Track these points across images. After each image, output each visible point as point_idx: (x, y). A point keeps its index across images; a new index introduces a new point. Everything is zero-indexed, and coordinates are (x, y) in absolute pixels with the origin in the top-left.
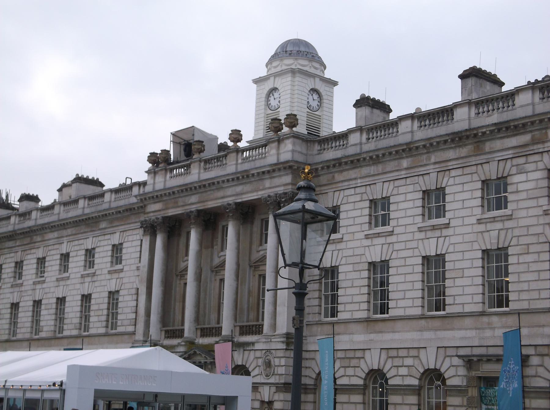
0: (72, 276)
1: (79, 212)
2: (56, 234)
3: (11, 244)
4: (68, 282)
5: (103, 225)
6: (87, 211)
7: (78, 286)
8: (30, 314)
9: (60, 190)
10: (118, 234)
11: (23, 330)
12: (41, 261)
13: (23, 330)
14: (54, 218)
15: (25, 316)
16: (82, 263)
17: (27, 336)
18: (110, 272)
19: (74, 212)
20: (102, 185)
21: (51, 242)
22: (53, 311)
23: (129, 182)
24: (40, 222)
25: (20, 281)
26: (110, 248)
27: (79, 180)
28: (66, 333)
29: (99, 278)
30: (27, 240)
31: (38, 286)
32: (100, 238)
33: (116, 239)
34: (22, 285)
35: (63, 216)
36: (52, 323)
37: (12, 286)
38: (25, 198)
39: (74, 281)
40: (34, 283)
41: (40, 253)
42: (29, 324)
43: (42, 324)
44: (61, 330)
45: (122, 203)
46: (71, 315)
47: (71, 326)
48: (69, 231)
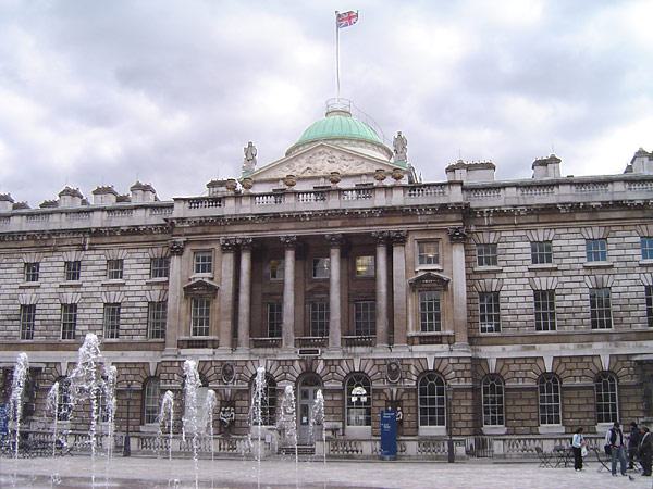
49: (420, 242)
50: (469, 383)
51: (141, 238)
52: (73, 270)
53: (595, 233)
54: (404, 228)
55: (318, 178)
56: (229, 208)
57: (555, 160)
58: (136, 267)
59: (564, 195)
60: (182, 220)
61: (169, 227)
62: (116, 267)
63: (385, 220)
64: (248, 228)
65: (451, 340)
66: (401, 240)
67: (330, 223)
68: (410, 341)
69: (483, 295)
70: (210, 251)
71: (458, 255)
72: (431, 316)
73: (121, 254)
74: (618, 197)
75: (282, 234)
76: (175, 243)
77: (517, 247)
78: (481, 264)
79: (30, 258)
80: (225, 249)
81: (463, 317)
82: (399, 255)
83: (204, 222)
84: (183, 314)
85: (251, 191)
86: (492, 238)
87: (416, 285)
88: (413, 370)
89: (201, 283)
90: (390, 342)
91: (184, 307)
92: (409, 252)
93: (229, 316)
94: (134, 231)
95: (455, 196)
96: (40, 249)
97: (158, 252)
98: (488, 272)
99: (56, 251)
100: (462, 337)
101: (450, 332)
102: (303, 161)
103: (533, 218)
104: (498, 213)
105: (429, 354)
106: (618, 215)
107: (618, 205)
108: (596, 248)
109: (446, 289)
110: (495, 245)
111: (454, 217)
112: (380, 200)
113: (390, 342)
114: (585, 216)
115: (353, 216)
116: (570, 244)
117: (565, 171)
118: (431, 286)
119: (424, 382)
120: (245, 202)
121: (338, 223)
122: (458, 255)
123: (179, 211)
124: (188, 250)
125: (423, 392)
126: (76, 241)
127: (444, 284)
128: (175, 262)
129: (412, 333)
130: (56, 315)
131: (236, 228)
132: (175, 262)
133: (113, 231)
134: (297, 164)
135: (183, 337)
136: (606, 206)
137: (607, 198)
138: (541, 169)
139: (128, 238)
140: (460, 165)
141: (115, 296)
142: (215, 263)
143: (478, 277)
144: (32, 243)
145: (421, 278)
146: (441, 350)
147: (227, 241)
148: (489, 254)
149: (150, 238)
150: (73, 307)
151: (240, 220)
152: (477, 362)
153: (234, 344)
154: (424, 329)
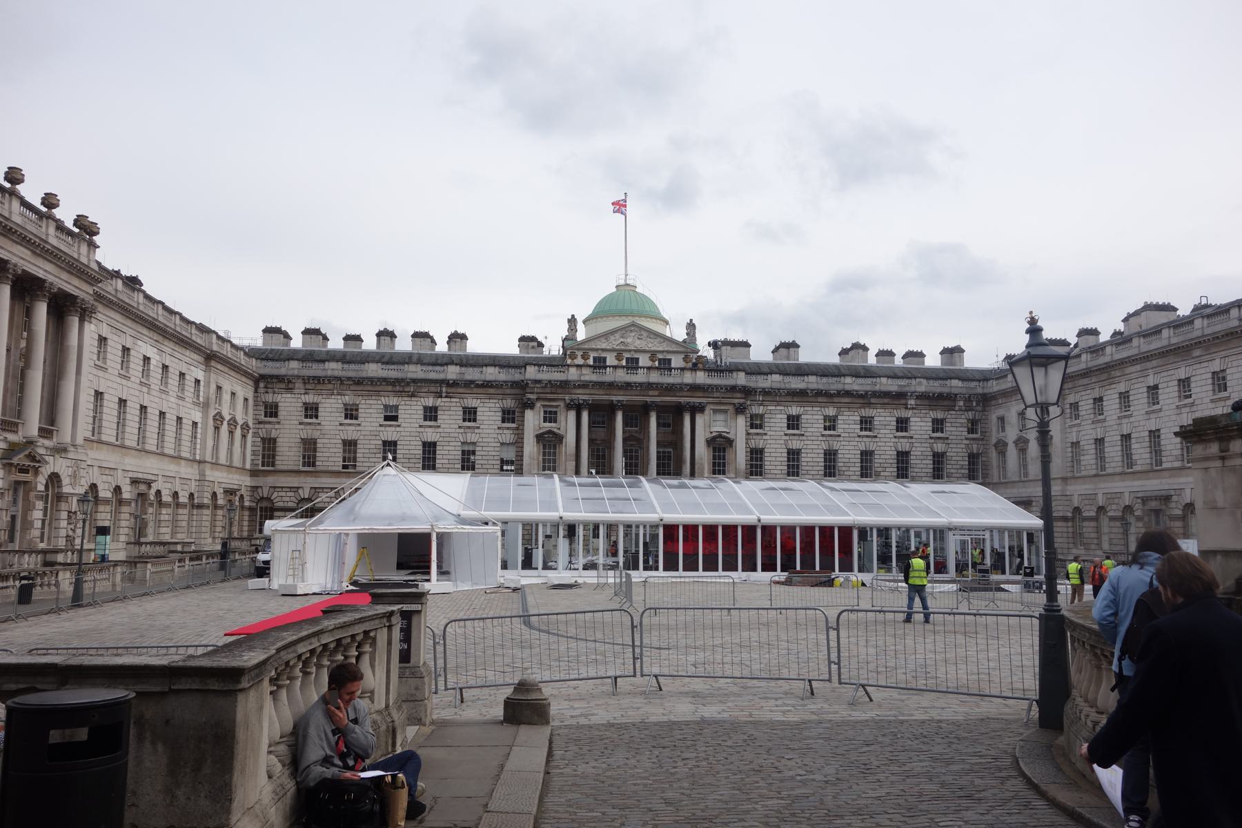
0: (1165, 408)
1: (1165, 343)
2: (1138, 367)
3: (1085, 381)
4: (1161, 414)
5: (1197, 353)
6: (1174, 340)
7: (1174, 417)
8: (1119, 448)
9: (1125, 320)
10: (1217, 361)
11: (1113, 465)
12: (1124, 397)
13: (1113, 465)
14: (1135, 351)
15: (1113, 451)
16: (1176, 394)
17: (1119, 470)
18: (1212, 401)
19: (1156, 344)
20: (1175, 309)
21: (1133, 376)
22: (1147, 444)
23: (1204, 302)
24: (1118, 356)
25: (1101, 417)
26: (1210, 375)
27: (1148, 307)
28: (1165, 466)
29: (1200, 407)
30: (1105, 376)
31: (1124, 421)
32: (1198, 366)
33: (1216, 366)
34: (1104, 420)
35: (1144, 348)
36: (1148, 456)
37: (1093, 423)
38: (1083, 333)
39: (1168, 413)
40: (1119, 418)
41: (1122, 388)
42: (1120, 459)
43: (1134, 457)
44: (1159, 463)
45: (1218, 328)
46: (1169, 447)
47: (1170, 459)
48: (1154, 363)
51: (492, 391)
52: (431, 414)
53: (831, 411)
54: (704, 400)
55: (630, 351)
56: (573, 374)
57: (793, 345)
58: (489, 412)
59: (812, 382)
61: (521, 386)
62: (470, 414)
64: (587, 391)
66: (700, 409)
67: (651, 393)
70: (557, 407)
71: (741, 421)
73: (472, 402)
74: (848, 388)
75: (614, 398)
77: (777, 418)
78: (752, 427)
79: (393, 401)
80: (569, 407)
82: (700, 420)
86: (761, 410)
87: (710, 442)
89: (550, 432)
92: (707, 418)
94: (487, 385)
95: (741, 379)
96: (399, 394)
97: (509, 403)
99: (413, 396)
102: (618, 335)
103: (789, 398)
104: (766, 392)
106: (846, 400)
107: (848, 394)
108: (831, 423)
110: (762, 416)
111: (739, 395)
112: (688, 378)
114: (825, 400)
115: (670, 389)
116: (813, 418)
117: (805, 356)
118: (720, 445)
120: (585, 371)
121: (656, 393)
122: (741, 421)
123: (531, 373)
124: (538, 405)
126: (432, 389)
127: (730, 442)
128: (529, 414)
130: (419, 451)
132: (529, 414)
133: (469, 384)
136: (840, 394)
137: (840, 387)
138: (783, 351)
139: (480, 390)
140: (727, 343)
141: (471, 437)
144: (390, 388)
145: (714, 438)
148: (756, 423)
149: (500, 391)
150: (434, 444)
151: (584, 385)
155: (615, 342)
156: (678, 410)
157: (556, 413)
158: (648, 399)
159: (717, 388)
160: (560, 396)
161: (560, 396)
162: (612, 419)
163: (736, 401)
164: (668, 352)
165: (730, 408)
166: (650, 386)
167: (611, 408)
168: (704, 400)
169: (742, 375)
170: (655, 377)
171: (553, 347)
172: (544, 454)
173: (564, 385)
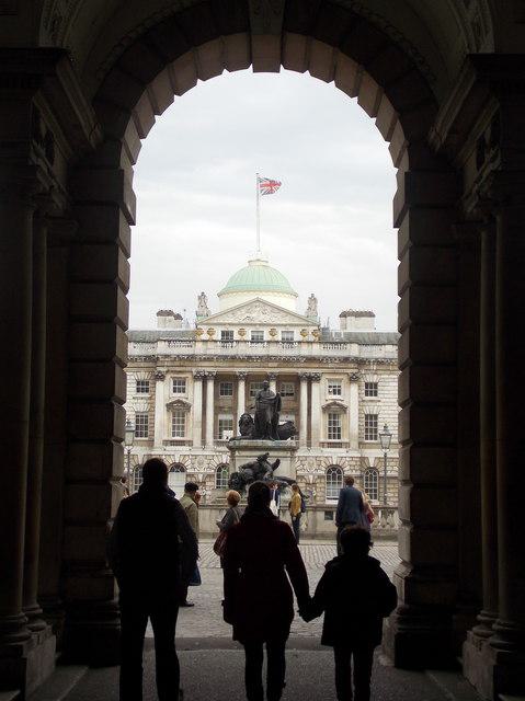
49: (330, 380)
50: (358, 473)
54: (320, 371)
55: (255, 325)
56: (199, 349)
60: (166, 356)
63: (306, 365)
65: (347, 445)
66: (317, 378)
67: (270, 365)
68: (322, 445)
69: (367, 416)
71: (354, 388)
72: (335, 431)
75: (237, 370)
76: (159, 372)
78: (367, 395)
80: (196, 378)
81: (356, 431)
82: (315, 387)
83: (179, 358)
84: (166, 423)
85: (214, 337)
87: (326, 409)
88: (323, 464)
89: (179, 401)
90: (309, 445)
91: (166, 417)
92: (323, 387)
93: (200, 425)
95: (354, 351)
98: (372, 401)
100: (354, 444)
101: (346, 440)
102: (243, 311)
104: (379, 362)
105: (335, 455)
109: (345, 412)
112: (305, 351)
113: (309, 445)
115: (287, 361)
119: (329, 472)
120: (210, 345)
121: (276, 364)
123: (162, 348)
124: (168, 377)
125: (328, 478)
127: (344, 409)
129: (322, 440)
131: (206, 364)
132: (159, 385)
134: (239, 313)
135: (166, 438)
142: (189, 386)
143: (365, 404)
146: (341, 452)
147: (198, 372)
148: (372, 389)
151: (209, 359)
152: (363, 459)
153: (204, 442)
154: (330, 437)
155: (241, 317)
156: (297, 379)
157: (184, 384)
158: (269, 371)
159: (332, 359)
160: (187, 369)
161: (187, 369)
162: (237, 388)
163: (349, 371)
164: (291, 325)
165: (345, 378)
166: (269, 358)
167: (235, 379)
168: (320, 371)
169: (355, 346)
170: (274, 350)
171: (190, 320)
172: (174, 420)
173: (191, 358)
